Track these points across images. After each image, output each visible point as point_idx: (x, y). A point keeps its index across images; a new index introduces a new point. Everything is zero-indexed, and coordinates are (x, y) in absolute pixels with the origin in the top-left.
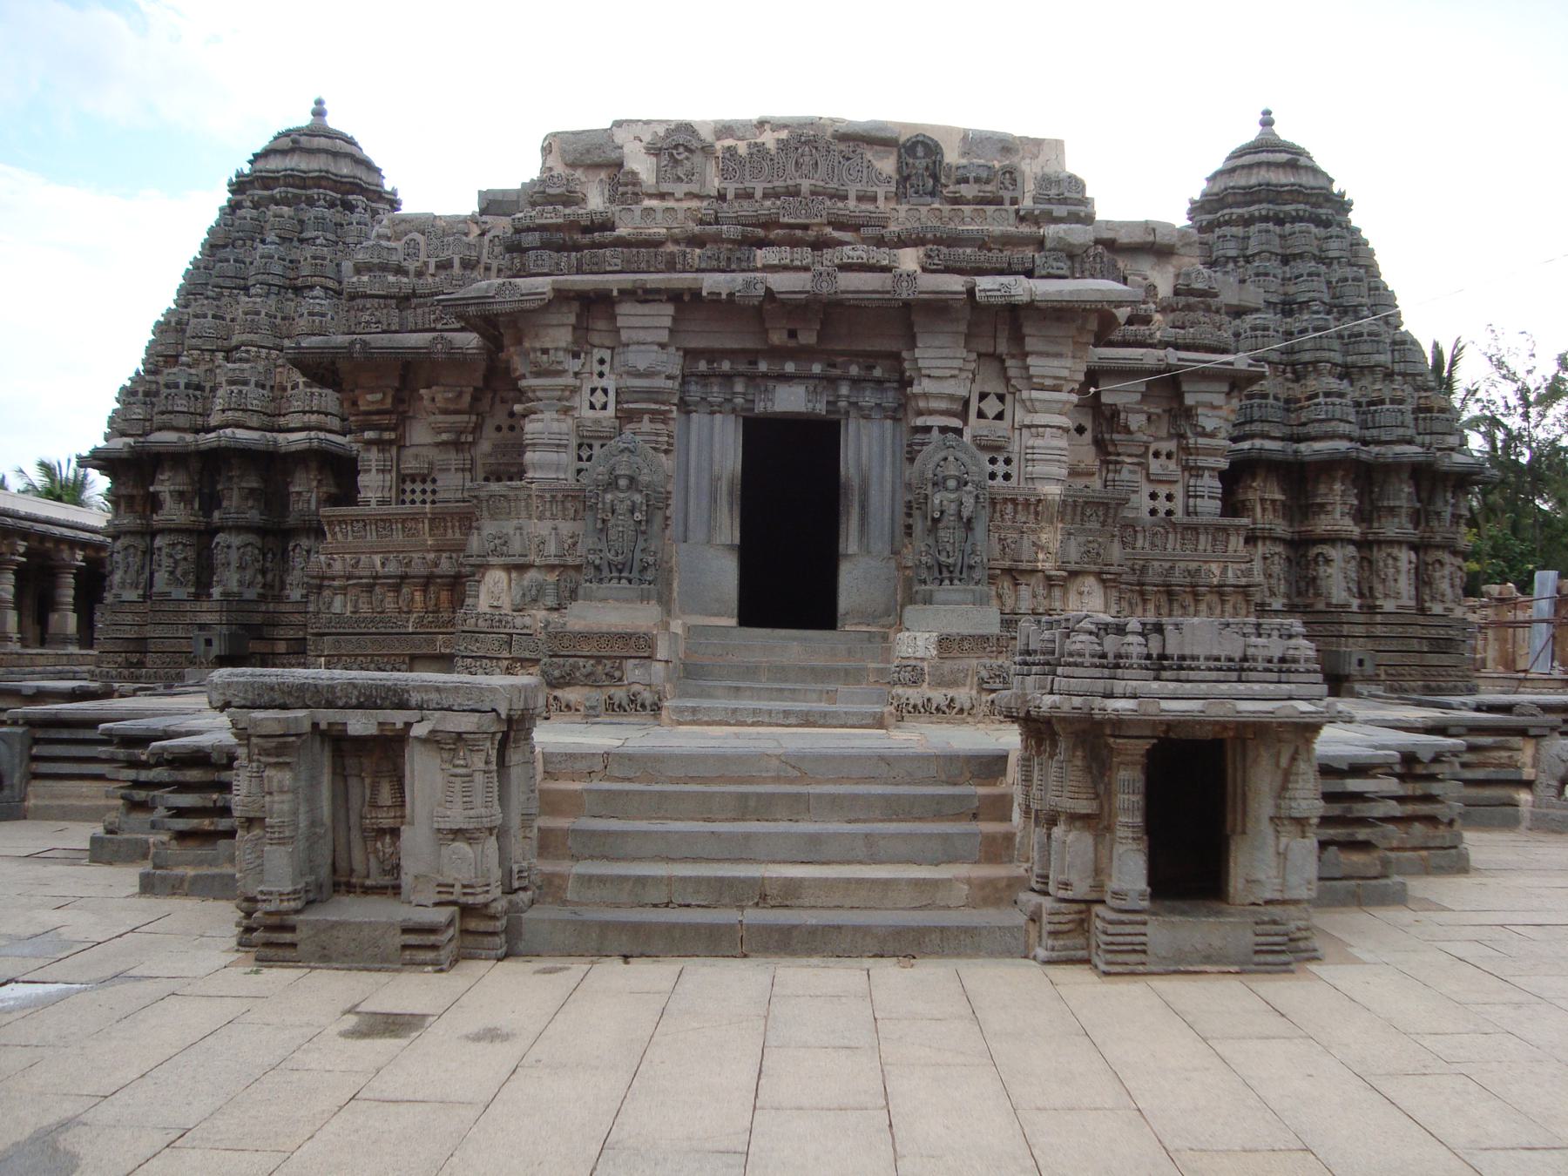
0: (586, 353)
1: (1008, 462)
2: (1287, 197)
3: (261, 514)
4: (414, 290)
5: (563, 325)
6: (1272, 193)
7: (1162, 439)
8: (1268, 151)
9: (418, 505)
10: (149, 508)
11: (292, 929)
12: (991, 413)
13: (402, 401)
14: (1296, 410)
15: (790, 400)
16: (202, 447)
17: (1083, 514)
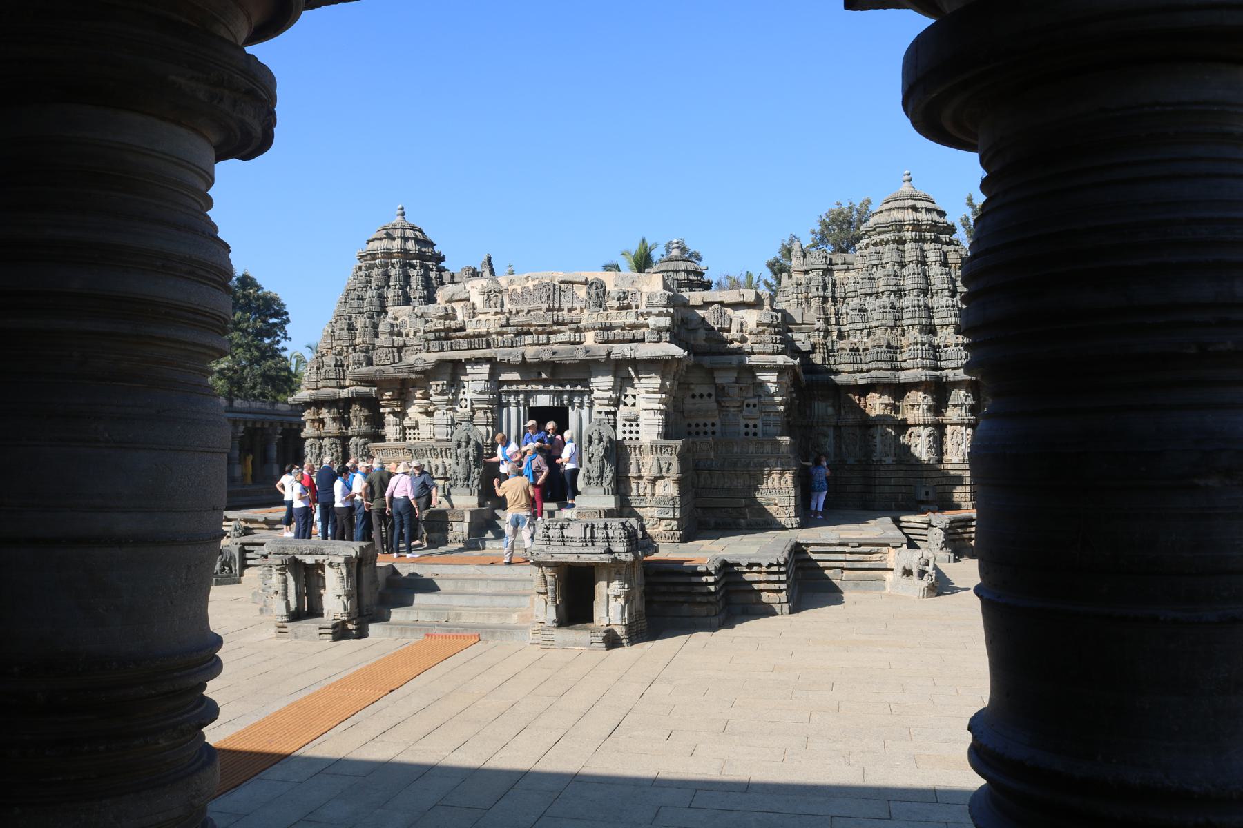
0: (457, 385)
1: (638, 425)
2: (907, 227)
3: (372, 428)
4: (405, 343)
5: (445, 373)
6: (899, 226)
7: (750, 398)
8: (901, 200)
9: (412, 440)
10: (321, 426)
11: (286, 627)
12: (630, 404)
13: (402, 394)
14: (901, 353)
15: (543, 401)
16: (342, 397)
17: (661, 451)
